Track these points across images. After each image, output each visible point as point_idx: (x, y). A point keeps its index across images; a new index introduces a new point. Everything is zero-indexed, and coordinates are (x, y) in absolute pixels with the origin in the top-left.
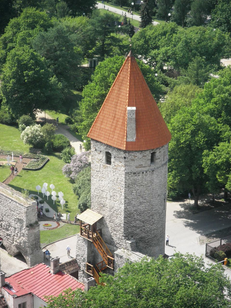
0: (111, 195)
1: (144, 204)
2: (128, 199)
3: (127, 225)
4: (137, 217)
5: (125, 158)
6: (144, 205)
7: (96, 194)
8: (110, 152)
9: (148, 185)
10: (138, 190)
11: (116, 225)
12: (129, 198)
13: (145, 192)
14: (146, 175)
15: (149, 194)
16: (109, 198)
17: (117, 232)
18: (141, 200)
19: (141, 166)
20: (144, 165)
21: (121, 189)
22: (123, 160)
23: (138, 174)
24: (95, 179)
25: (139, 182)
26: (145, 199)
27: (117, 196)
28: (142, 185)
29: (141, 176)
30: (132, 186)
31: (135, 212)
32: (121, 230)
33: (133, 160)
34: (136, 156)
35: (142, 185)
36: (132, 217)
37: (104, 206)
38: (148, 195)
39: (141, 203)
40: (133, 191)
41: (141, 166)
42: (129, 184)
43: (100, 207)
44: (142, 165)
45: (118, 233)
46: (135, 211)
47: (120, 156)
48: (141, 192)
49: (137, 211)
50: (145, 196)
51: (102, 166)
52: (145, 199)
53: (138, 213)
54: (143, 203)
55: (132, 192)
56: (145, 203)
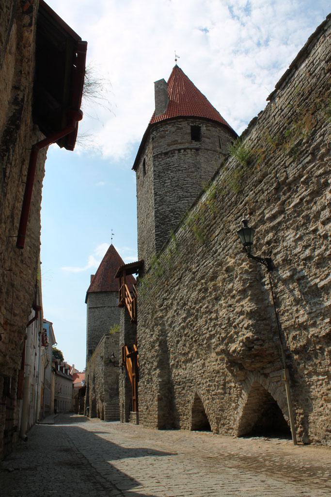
1: (185, 199)
2: (159, 195)
3: (160, 239)
4: (176, 222)
6: (187, 201)
9: (190, 170)
10: (174, 177)
12: (160, 193)
13: (186, 179)
14: (185, 154)
15: (194, 183)
18: (181, 193)
19: (175, 142)
20: (179, 141)
23: (172, 154)
25: (175, 166)
26: (186, 192)
28: (179, 170)
29: (176, 157)
30: (164, 173)
31: (171, 214)
33: (163, 137)
34: (167, 131)
35: (179, 170)
36: (168, 224)
38: (192, 185)
39: (180, 197)
40: (165, 180)
41: (175, 142)
42: (159, 172)
44: (177, 141)
46: (171, 211)
48: (178, 180)
49: (175, 212)
50: (187, 185)
52: (186, 192)
53: (177, 214)
54: (183, 198)
55: (165, 183)
56: (188, 197)
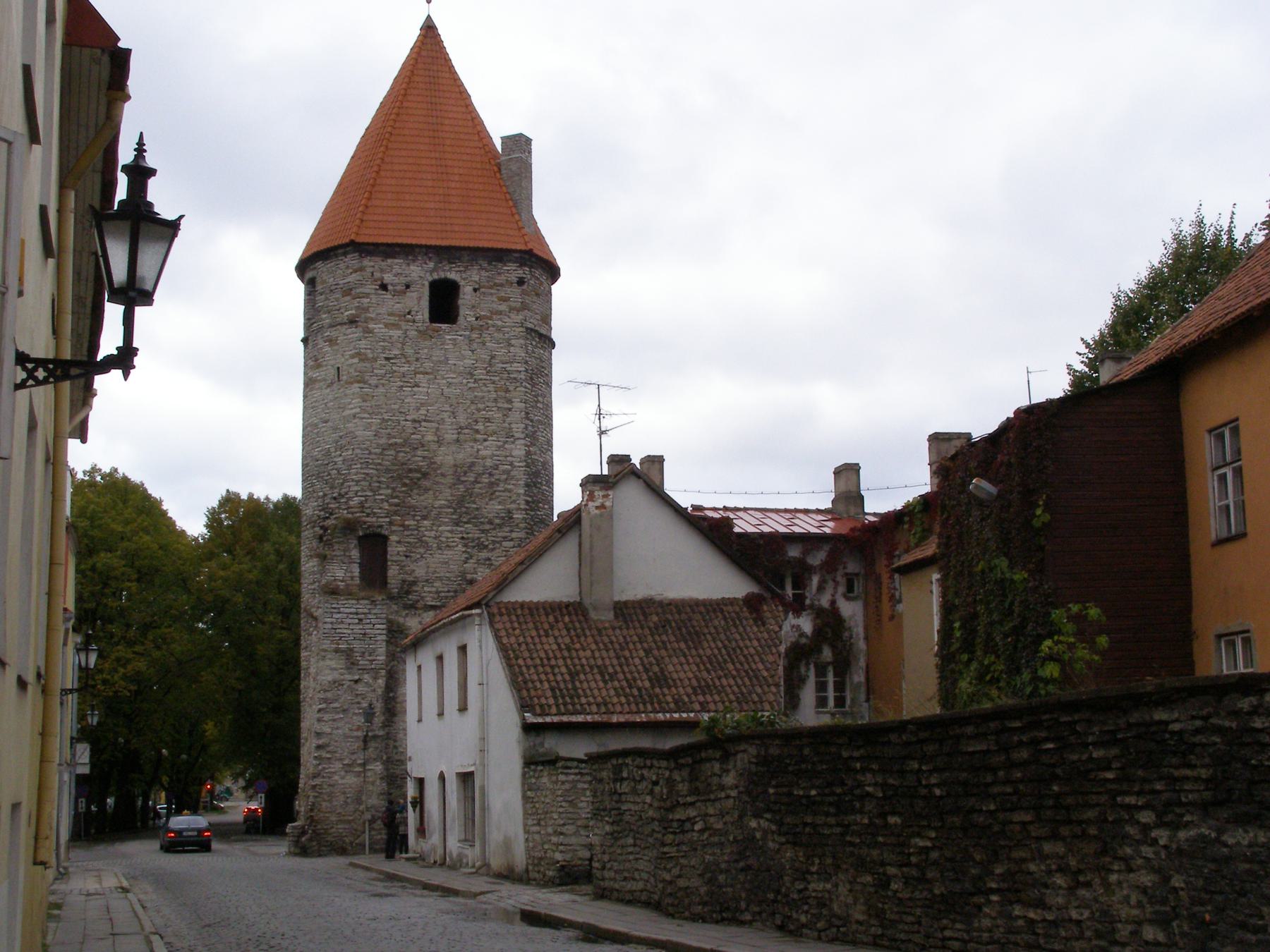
0: (462, 419)
5: (521, 282)
7: (383, 441)
8: (452, 276)
11: (487, 527)
16: (450, 436)
17: (493, 550)
21: (507, 391)
22: (514, 293)
24: (381, 390)
27: (488, 420)
32: (514, 535)
37: (425, 475)
43: (405, 485)
45: (496, 553)
47: (501, 279)
51: (413, 333)
